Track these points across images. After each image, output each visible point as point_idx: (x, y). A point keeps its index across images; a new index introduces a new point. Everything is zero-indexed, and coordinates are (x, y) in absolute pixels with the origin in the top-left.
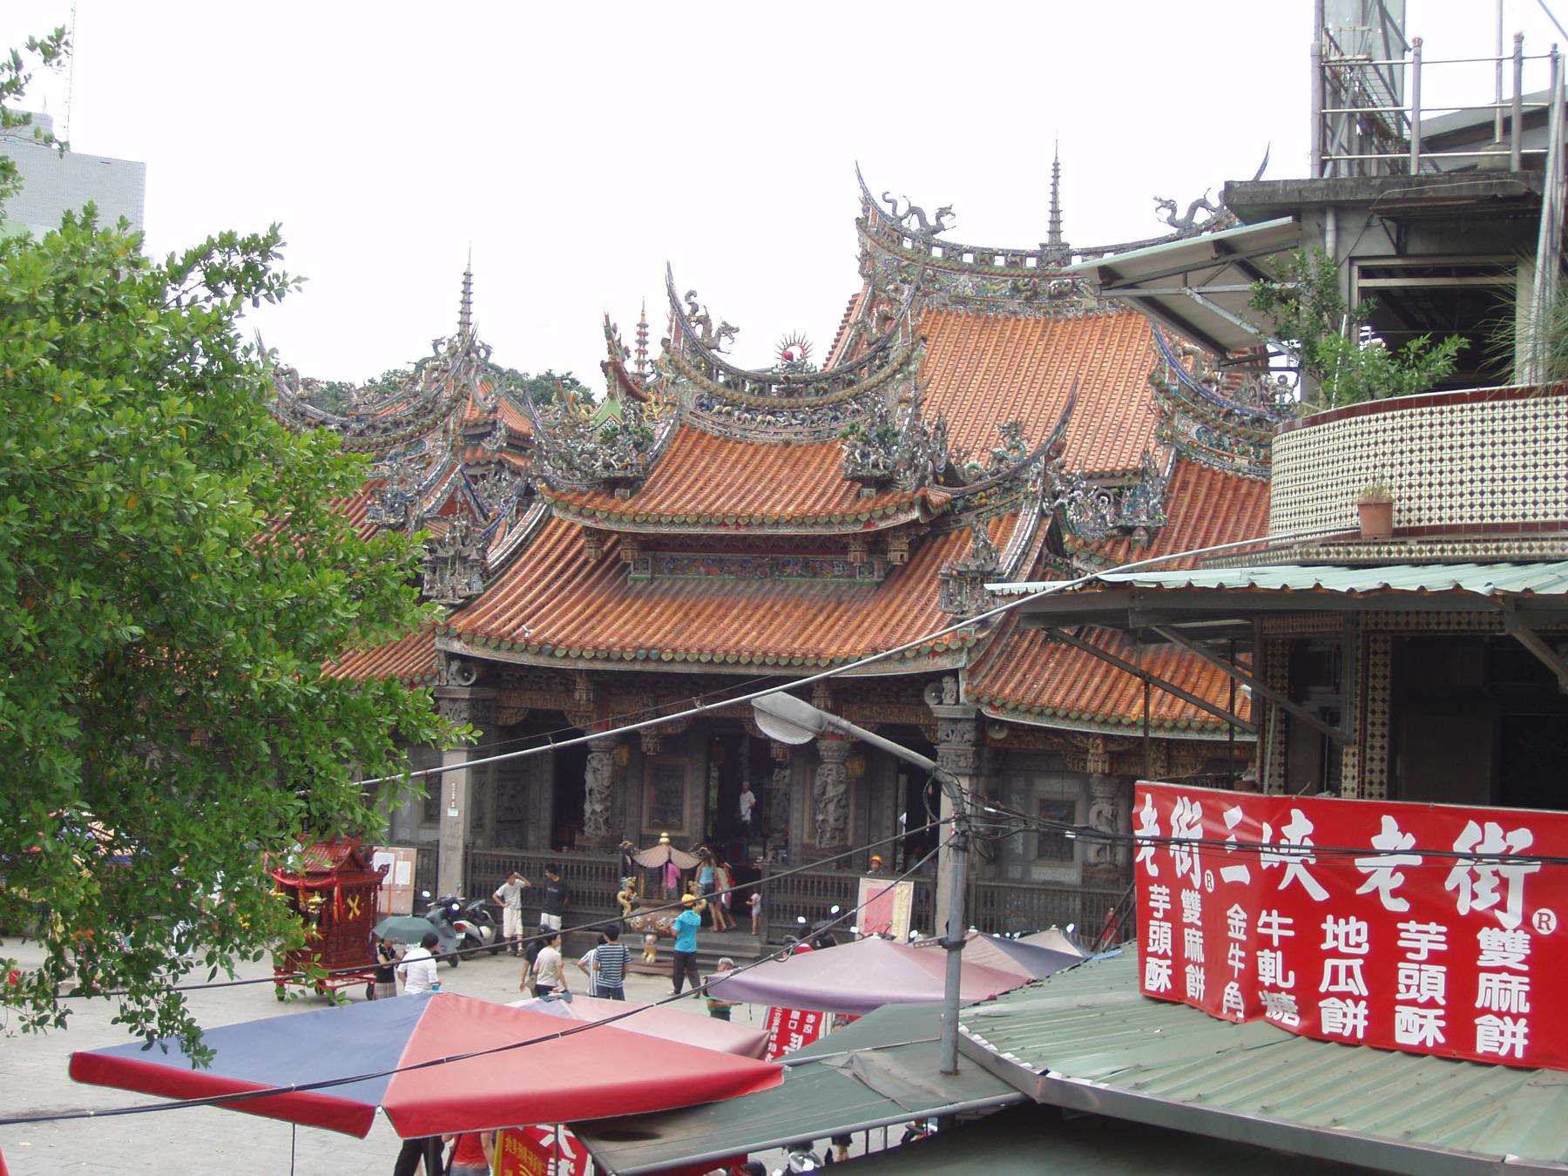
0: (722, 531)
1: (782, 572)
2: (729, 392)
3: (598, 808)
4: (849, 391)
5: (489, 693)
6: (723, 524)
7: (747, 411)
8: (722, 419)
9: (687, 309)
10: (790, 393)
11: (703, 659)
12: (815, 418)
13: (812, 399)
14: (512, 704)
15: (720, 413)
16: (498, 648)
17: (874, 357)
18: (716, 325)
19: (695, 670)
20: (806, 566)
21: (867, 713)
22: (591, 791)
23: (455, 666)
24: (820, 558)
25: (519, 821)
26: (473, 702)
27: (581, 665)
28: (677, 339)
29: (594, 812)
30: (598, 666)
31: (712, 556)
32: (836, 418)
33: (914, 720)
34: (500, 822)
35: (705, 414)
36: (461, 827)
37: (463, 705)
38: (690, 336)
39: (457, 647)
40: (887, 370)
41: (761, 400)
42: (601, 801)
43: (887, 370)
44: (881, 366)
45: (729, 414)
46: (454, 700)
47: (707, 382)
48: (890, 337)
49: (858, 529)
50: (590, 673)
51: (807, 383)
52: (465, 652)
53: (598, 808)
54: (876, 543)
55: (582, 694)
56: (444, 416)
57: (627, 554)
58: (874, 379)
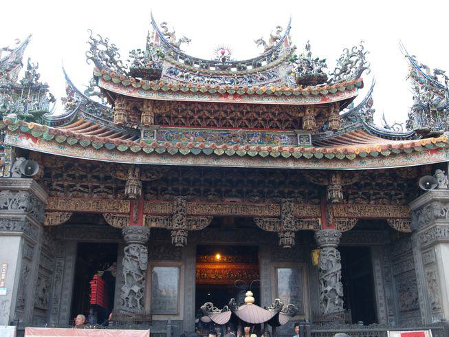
0: (223, 100)
1: (248, 140)
2: (187, 67)
3: (136, 289)
4: (257, 69)
5: (41, 194)
6: (227, 94)
7: (199, 76)
8: (182, 80)
9: (162, 30)
10: (223, 68)
11: (250, 153)
12: (240, 80)
13: (239, 72)
14: (59, 208)
15: (182, 76)
16: (65, 144)
17: (271, 55)
18: (178, 36)
19: (241, 164)
20: (263, 137)
21: (351, 210)
22: (129, 274)
23: (20, 161)
24: (273, 132)
25: (44, 310)
26: (32, 196)
27: (139, 160)
28: (157, 40)
29: (132, 292)
30: (153, 161)
31: (198, 130)
32: (250, 82)
33: (385, 215)
34: (36, 308)
35: (173, 77)
36: (8, 305)
37: (23, 195)
38: (163, 40)
39: (26, 143)
40: (278, 61)
41: (206, 71)
42: (140, 282)
43: (278, 61)
44: (275, 59)
45: (187, 77)
46: (15, 191)
47: (174, 61)
48: (278, 46)
49: (318, 101)
50: (143, 168)
51: (234, 64)
52: (31, 148)
53: (136, 289)
54: (322, 113)
55: (133, 188)
56: (8, 71)
57: (147, 118)
58: (271, 64)
